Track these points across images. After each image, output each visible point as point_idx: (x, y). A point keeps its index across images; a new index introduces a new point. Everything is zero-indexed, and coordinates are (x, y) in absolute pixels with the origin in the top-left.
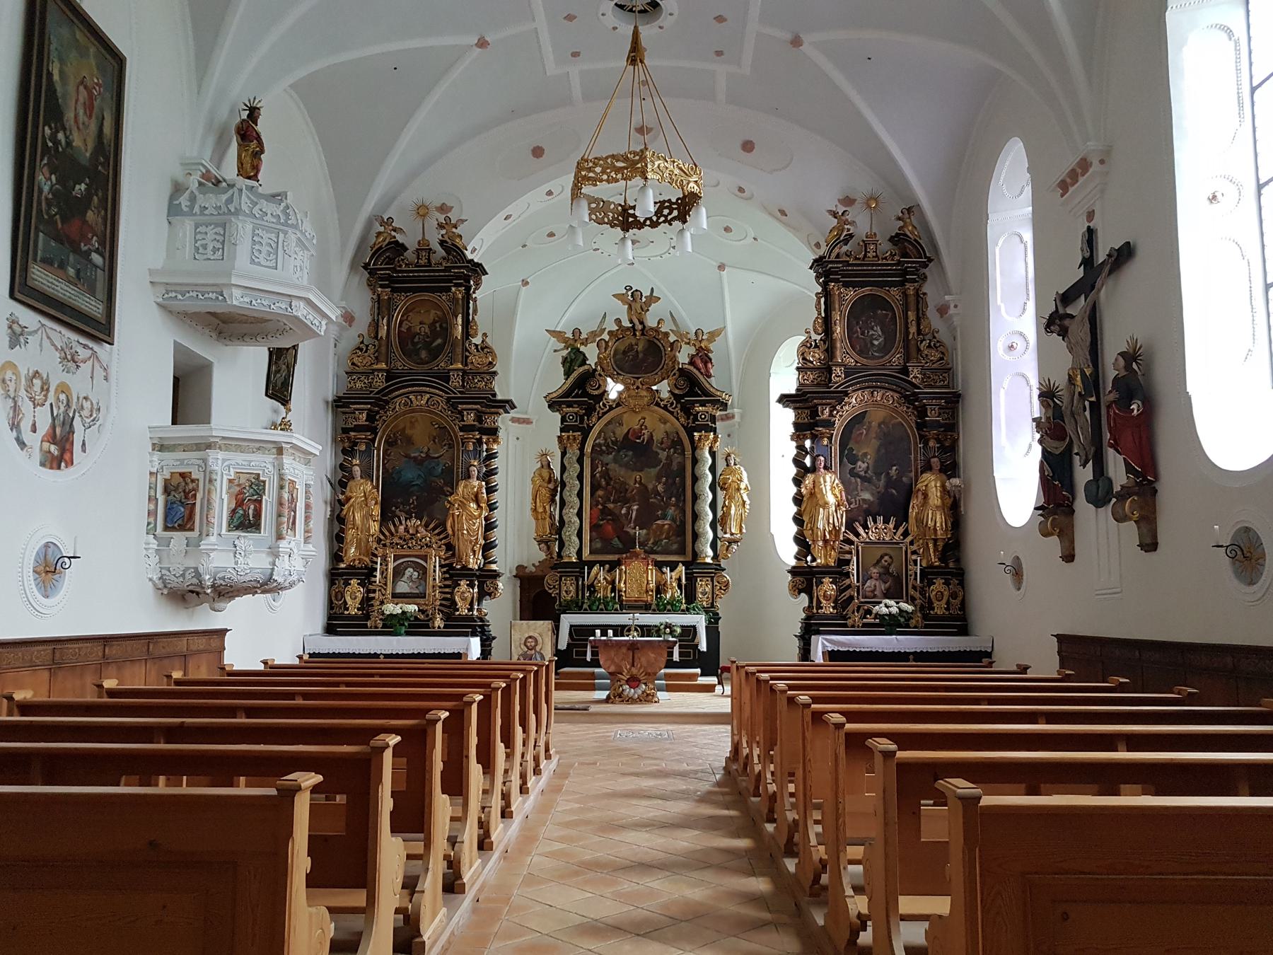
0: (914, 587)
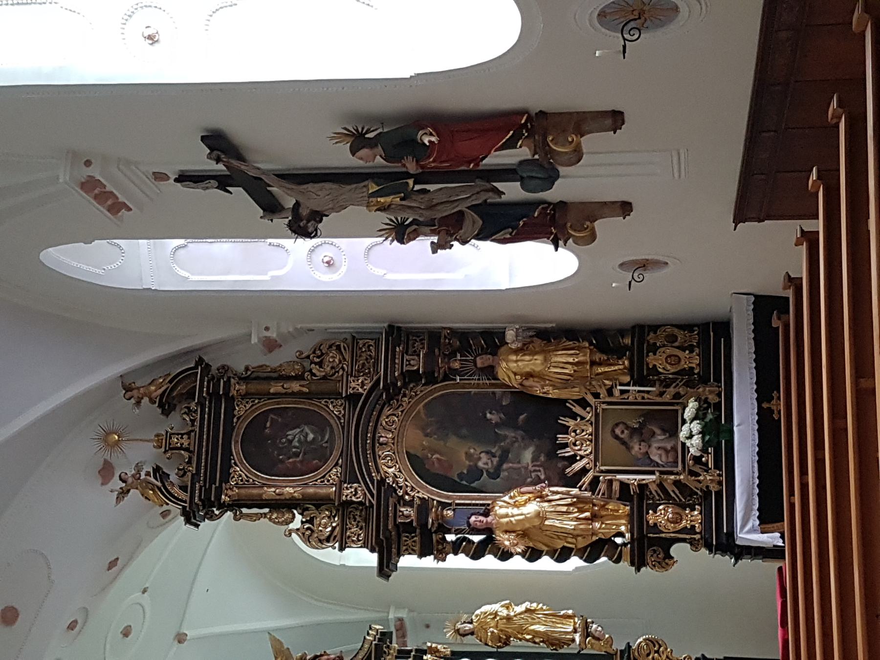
0: (661, 394)
